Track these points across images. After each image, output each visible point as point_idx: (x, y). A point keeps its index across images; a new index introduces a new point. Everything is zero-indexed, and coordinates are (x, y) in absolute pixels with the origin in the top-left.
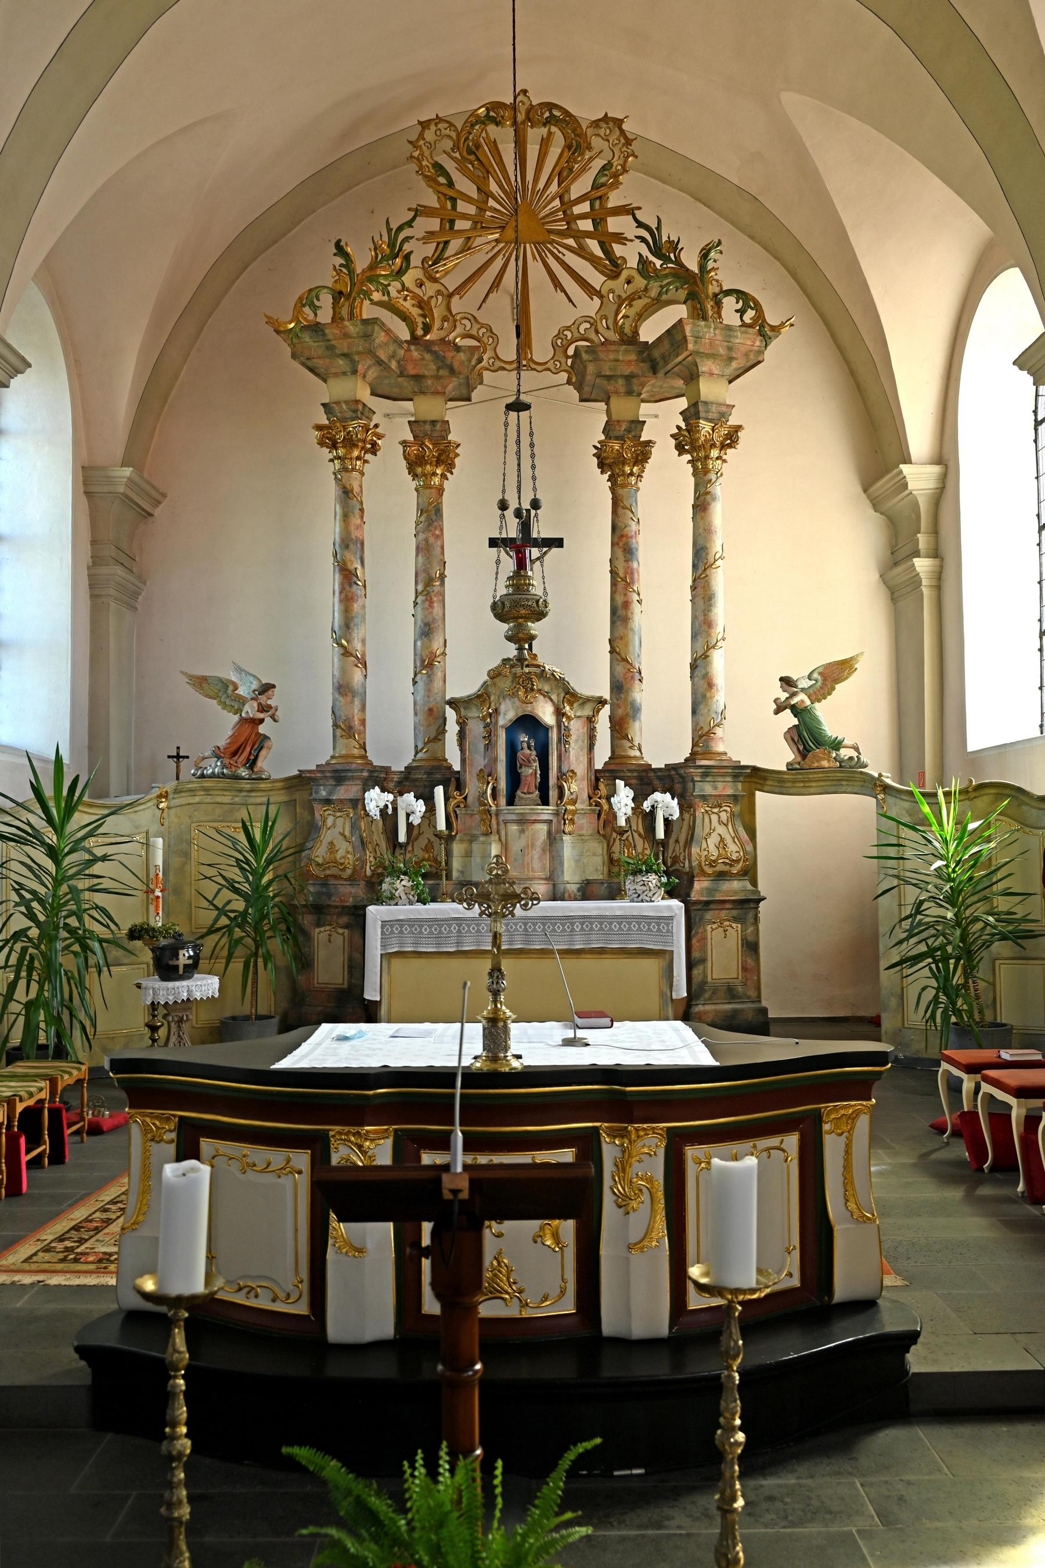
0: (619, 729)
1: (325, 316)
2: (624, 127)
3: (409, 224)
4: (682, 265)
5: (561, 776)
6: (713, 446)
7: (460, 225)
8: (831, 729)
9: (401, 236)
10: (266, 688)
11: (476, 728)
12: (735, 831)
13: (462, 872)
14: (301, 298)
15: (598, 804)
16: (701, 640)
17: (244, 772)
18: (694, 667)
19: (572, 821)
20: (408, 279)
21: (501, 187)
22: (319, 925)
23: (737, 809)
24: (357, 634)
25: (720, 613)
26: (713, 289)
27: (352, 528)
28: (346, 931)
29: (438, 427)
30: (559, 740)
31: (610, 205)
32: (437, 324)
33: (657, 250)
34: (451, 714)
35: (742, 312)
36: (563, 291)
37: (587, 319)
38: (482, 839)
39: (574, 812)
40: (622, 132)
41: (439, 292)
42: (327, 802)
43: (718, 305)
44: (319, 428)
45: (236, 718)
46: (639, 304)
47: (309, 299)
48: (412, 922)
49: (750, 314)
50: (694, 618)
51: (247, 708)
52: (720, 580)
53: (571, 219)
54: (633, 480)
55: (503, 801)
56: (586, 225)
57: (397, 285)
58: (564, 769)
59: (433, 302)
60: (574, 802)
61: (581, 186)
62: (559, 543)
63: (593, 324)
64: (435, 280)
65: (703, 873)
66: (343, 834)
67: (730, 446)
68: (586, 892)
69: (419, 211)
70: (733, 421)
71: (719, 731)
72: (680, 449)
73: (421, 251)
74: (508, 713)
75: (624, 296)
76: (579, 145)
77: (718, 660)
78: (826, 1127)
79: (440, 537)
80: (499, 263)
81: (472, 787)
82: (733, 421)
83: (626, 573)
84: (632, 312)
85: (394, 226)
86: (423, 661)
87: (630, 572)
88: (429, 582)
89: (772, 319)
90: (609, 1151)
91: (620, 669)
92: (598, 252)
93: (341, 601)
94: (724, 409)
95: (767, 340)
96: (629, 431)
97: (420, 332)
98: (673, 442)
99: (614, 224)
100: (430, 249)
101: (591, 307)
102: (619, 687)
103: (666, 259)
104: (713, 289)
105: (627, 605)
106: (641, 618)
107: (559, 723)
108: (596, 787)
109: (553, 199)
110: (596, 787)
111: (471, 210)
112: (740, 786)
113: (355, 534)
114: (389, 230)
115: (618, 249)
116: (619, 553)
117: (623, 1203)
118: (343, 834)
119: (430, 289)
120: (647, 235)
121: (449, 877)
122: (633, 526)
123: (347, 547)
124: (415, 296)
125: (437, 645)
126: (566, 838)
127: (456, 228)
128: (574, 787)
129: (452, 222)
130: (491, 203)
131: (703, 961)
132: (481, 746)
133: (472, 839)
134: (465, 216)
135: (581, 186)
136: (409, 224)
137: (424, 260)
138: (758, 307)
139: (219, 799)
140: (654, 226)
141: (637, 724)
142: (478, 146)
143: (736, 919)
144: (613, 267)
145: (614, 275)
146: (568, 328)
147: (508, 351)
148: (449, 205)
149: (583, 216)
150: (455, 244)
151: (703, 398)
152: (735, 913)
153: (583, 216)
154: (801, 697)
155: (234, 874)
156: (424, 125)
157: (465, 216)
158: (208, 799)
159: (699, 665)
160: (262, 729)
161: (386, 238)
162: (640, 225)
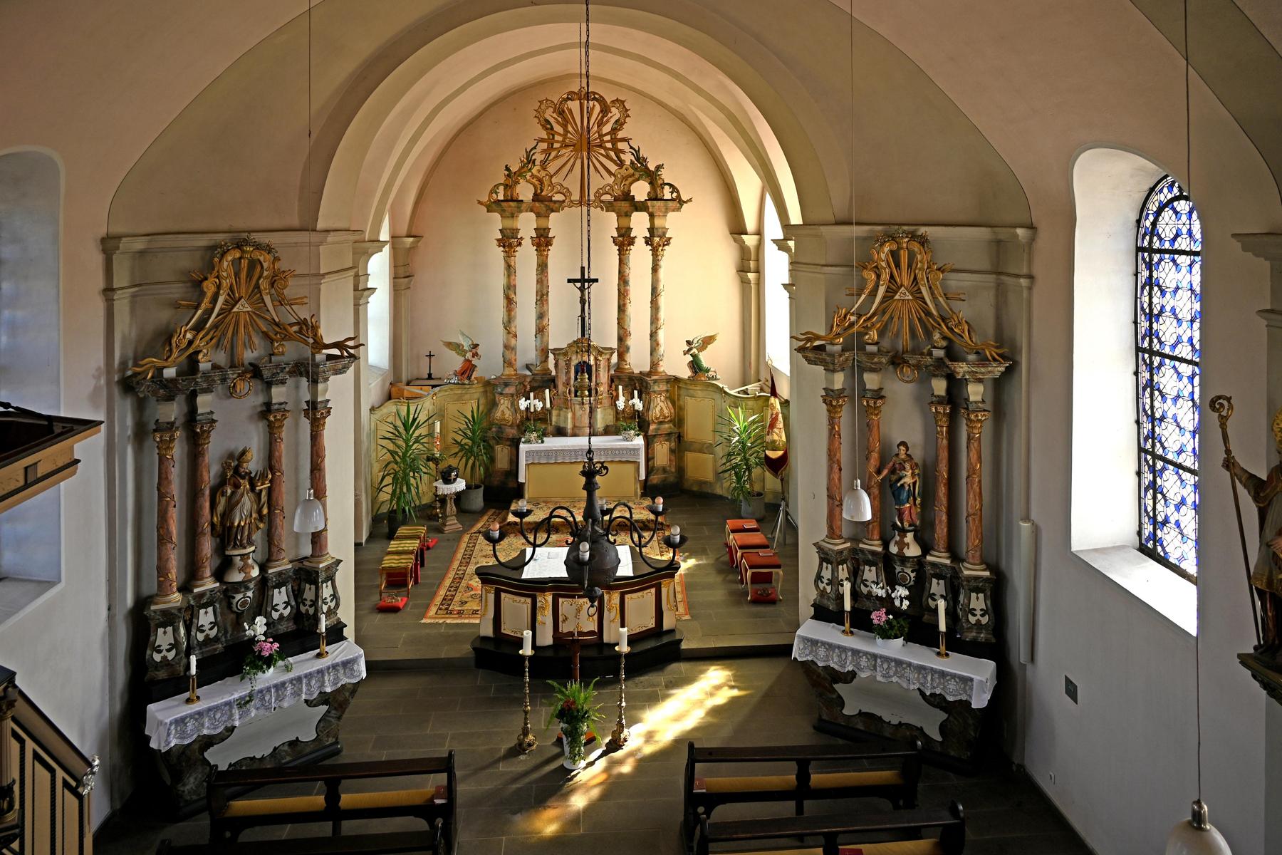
0: (621, 356)
1: (501, 197)
2: (625, 104)
3: (535, 148)
4: (648, 169)
5: (597, 384)
6: (660, 246)
7: (556, 145)
8: (705, 364)
9: (532, 153)
10: (476, 346)
11: (562, 363)
12: (667, 404)
13: (556, 422)
14: (491, 191)
15: (611, 394)
16: (654, 326)
17: (467, 382)
18: (651, 336)
19: (601, 403)
20: (534, 171)
21: (573, 128)
22: (498, 445)
23: (668, 395)
24: (513, 325)
25: (662, 314)
26: (660, 182)
27: (512, 281)
28: (509, 448)
29: (546, 231)
30: (596, 370)
31: (619, 137)
32: (546, 188)
33: (638, 158)
34: (551, 356)
35: (672, 193)
36: (599, 172)
37: (609, 185)
38: (564, 410)
39: (602, 399)
40: (624, 106)
41: (547, 175)
42: (501, 394)
43: (663, 188)
44: (498, 240)
45: (463, 358)
46: (630, 180)
47: (494, 191)
48: (537, 452)
49: (675, 195)
50: (652, 316)
51: (468, 355)
52: (662, 301)
53: (602, 142)
54: (627, 252)
55: (573, 395)
56: (609, 145)
57: (530, 174)
58: (598, 382)
59: (544, 179)
60: (602, 395)
61: (607, 128)
62: (596, 280)
63: (611, 187)
64: (544, 169)
65: (654, 422)
66: (508, 408)
67: (666, 245)
68: (607, 431)
69: (542, 140)
70: (668, 235)
71: (661, 363)
72: (647, 243)
73: (539, 157)
74: (575, 361)
75: (624, 175)
76: (606, 111)
77: (661, 335)
78: (662, 586)
79: (547, 276)
80: (572, 160)
81: (561, 388)
82: (668, 235)
83: (624, 292)
84: (627, 183)
85: (528, 150)
86: (539, 329)
87: (627, 291)
88: (542, 295)
89: (684, 198)
90: (606, 597)
91: (621, 331)
92: (615, 158)
93: (507, 311)
94: (664, 230)
95: (682, 205)
96: (626, 232)
97: (539, 191)
98: (644, 240)
99: (621, 145)
100: (542, 157)
101: (611, 180)
102: (621, 339)
104: (660, 182)
105: (624, 305)
106: (631, 309)
108: (611, 387)
109: (595, 133)
110: (611, 387)
111: (560, 138)
112: (669, 385)
114: (527, 152)
115: (622, 156)
116: (622, 283)
117: (609, 610)
118: (508, 408)
119: (543, 173)
120: (634, 152)
121: (551, 424)
122: (627, 271)
123: (509, 289)
124: (537, 177)
125: (545, 322)
126: (598, 410)
127: (554, 147)
128: (602, 389)
129: (552, 144)
130: (569, 135)
131: (653, 458)
132: (565, 371)
133: (560, 409)
134: (557, 142)
135: (607, 128)
136: (535, 148)
137: (541, 161)
138: (678, 192)
139: (457, 392)
140: (637, 149)
141: (628, 355)
142: (564, 111)
143: (666, 441)
144: (621, 164)
148: (551, 137)
149: (608, 142)
150: (553, 154)
151: (656, 226)
152: (666, 438)
153: (608, 142)
154: (695, 350)
155: (468, 432)
156: (541, 102)
157: (557, 142)
158: (452, 393)
159: (653, 335)
160: (473, 363)
161: (525, 156)
162: (631, 148)
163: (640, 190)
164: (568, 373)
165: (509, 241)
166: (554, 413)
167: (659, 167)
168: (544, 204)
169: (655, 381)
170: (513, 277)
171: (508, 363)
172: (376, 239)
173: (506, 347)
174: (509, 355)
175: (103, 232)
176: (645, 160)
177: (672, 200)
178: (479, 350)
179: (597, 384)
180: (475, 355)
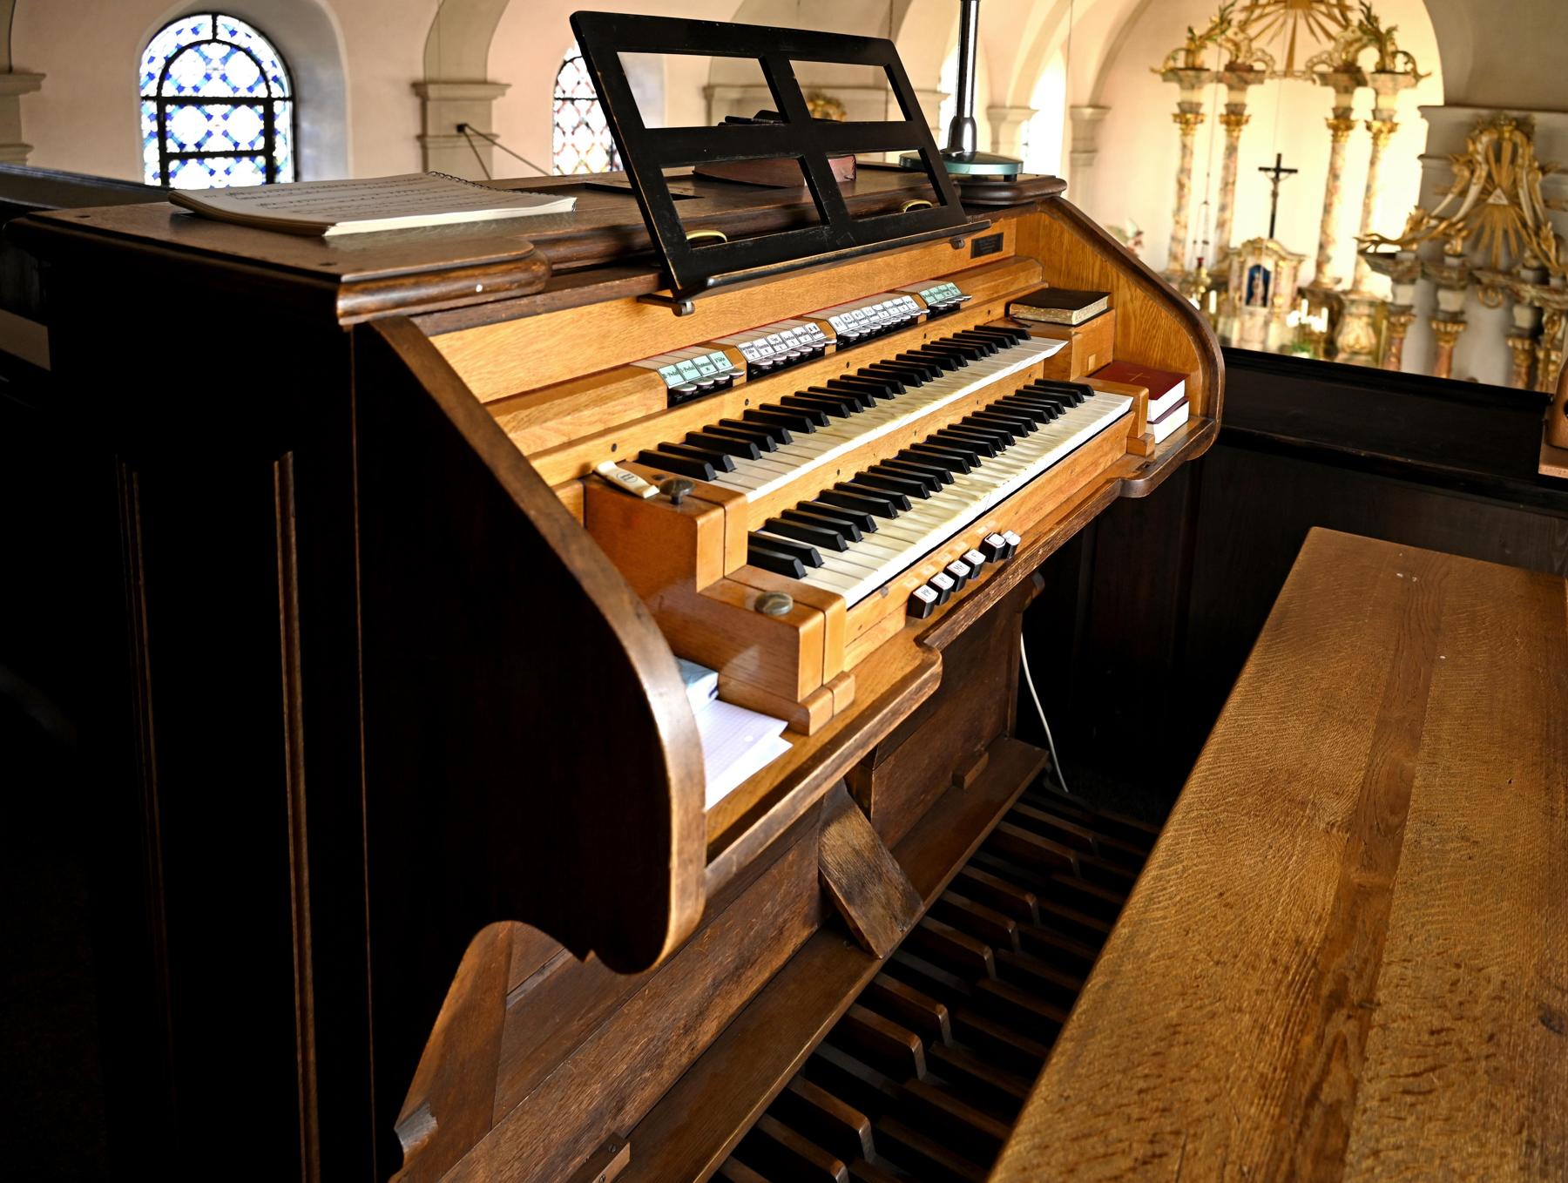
46: (1356, 46)
55: (1243, 302)
58: (1278, 291)
74: (1251, 262)
81: (1231, 293)
101: (1329, 45)
103: (1372, 25)
107: (1276, 271)
113: (1187, 166)
119: (1241, 36)
120: (1364, 9)
144: (1346, 24)
145: (1345, 27)
146: (1316, 57)
147: (1280, 66)
163: (1368, 59)
164: (1241, 276)
165: (1187, 115)
166: (1221, 320)
167: (1390, 31)
168: (1239, 74)
169: (1353, 302)
170: (1187, 159)
171: (1174, 257)
172: (1023, 104)
173: (1174, 239)
174: (1178, 249)
175: (704, 81)
176: (1376, 19)
177: (1406, 73)
178: (1144, 238)
179: (1275, 295)
180: (1138, 243)
